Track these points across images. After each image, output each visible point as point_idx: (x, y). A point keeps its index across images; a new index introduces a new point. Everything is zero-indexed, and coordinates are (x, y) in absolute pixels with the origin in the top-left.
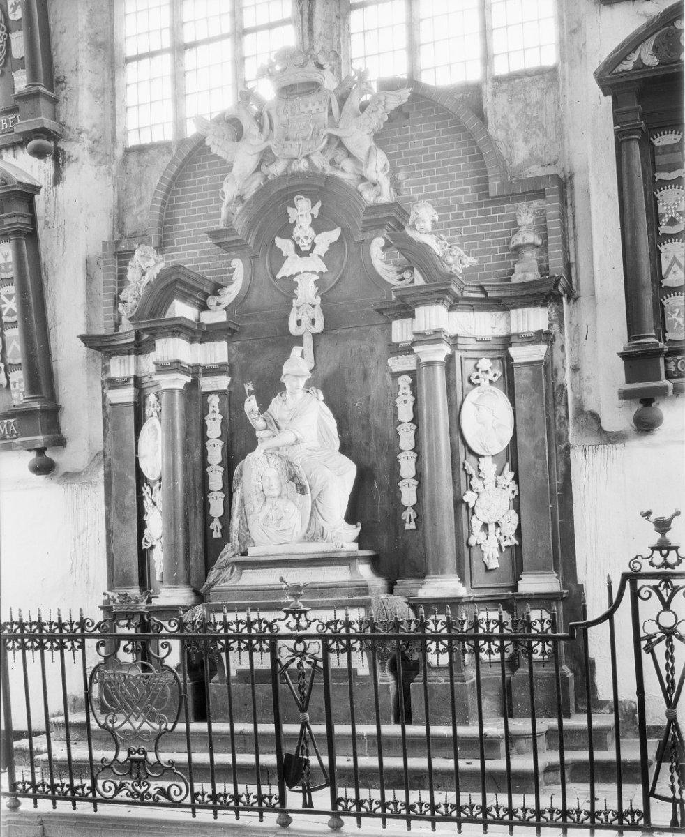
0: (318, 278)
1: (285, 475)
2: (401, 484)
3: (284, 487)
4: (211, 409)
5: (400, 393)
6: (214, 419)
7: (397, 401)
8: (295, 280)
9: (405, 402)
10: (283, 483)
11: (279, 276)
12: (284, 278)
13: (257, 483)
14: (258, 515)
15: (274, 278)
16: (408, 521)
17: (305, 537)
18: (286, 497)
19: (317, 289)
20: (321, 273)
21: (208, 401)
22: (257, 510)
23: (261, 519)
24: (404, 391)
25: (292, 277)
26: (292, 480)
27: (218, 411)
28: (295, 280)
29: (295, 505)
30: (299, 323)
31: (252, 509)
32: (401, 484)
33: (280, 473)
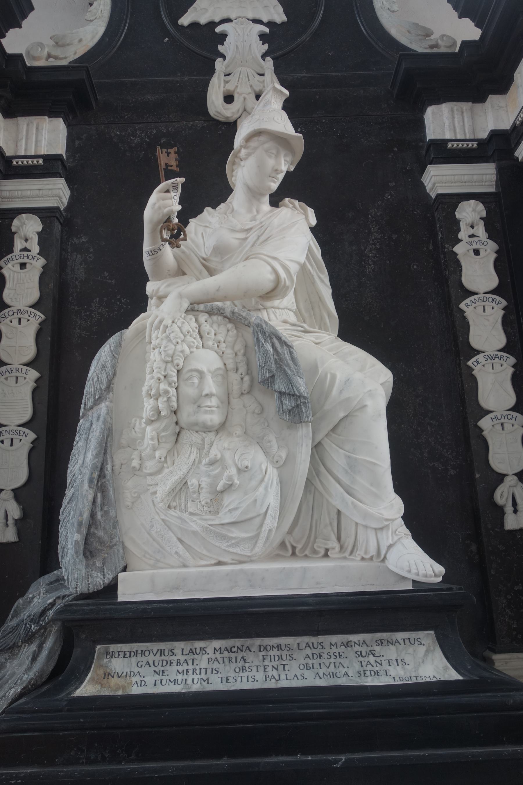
0: (267, 30)
1: (242, 369)
2: (485, 423)
3: (236, 402)
4: (18, 244)
5: (462, 235)
6: (23, 266)
7: (458, 249)
8: (218, 30)
9: (477, 252)
10: (236, 388)
11: (185, 21)
12: (195, 25)
13: (163, 386)
14: (150, 480)
15: (175, 23)
16: (509, 509)
17: (283, 545)
18: (239, 431)
19: (266, 46)
20: (270, 24)
21: (13, 229)
22: (150, 466)
23: (159, 495)
24: (471, 231)
25: (212, 25)
26: (269, 381)
27: (36, 249)
28: (218, 29)
29: (266, 453)
30: (229, 99)
31: (135, 463)
32: (485, 423)
33: (231, 365)
